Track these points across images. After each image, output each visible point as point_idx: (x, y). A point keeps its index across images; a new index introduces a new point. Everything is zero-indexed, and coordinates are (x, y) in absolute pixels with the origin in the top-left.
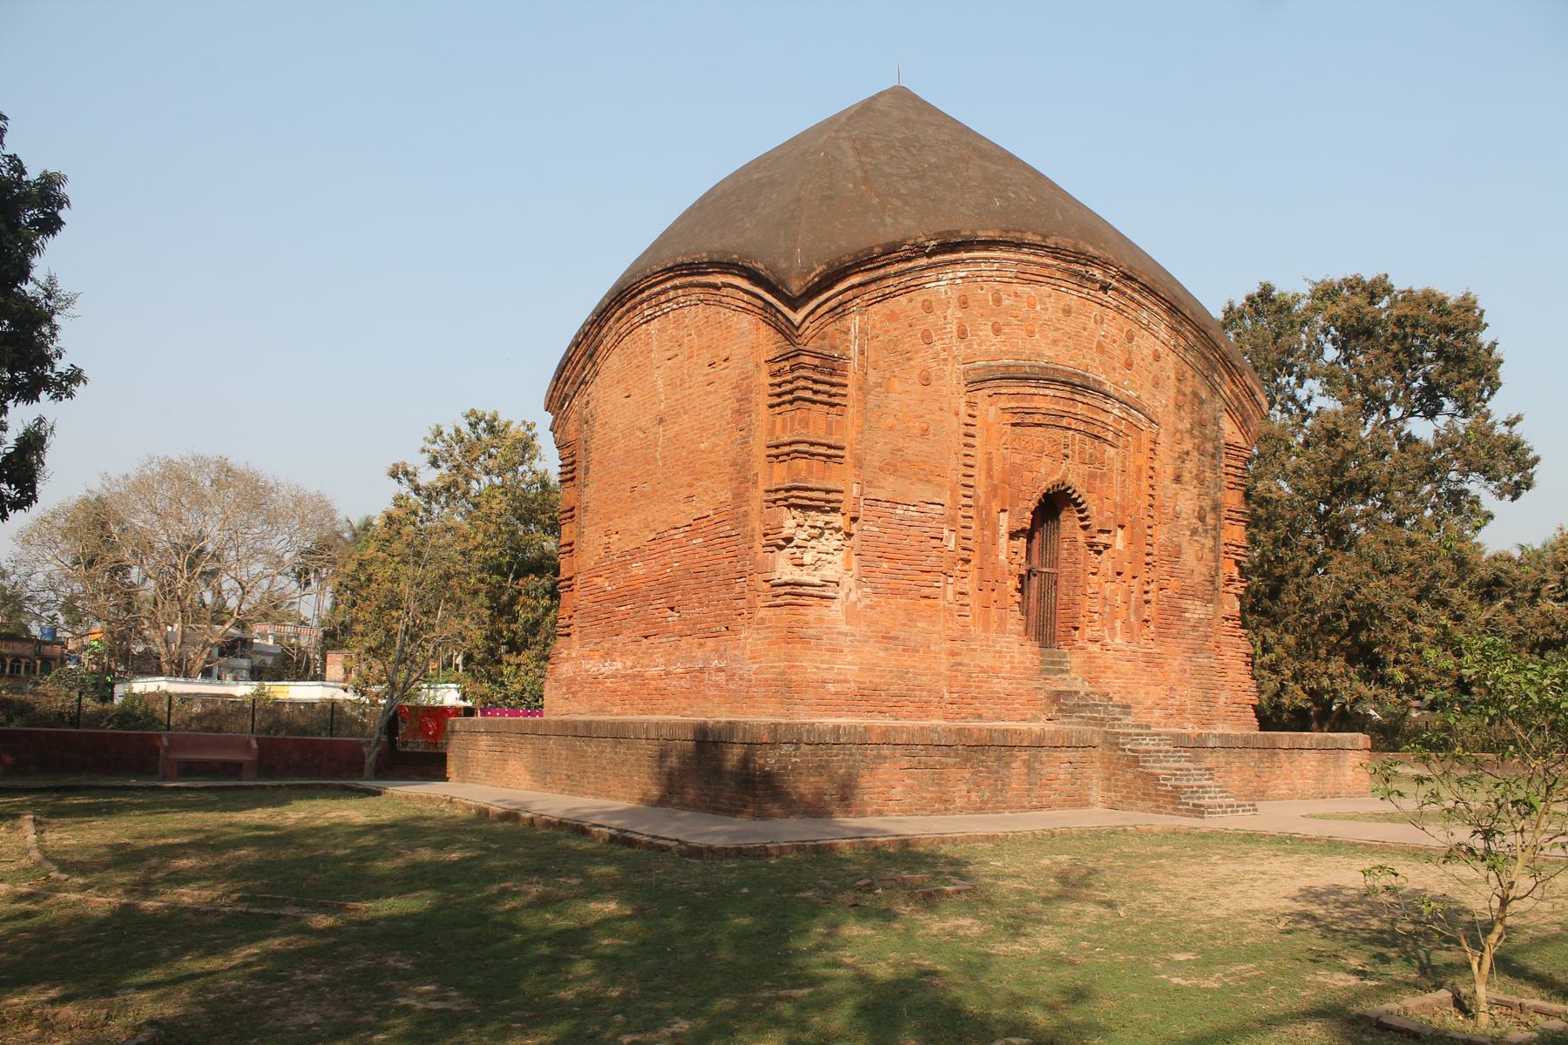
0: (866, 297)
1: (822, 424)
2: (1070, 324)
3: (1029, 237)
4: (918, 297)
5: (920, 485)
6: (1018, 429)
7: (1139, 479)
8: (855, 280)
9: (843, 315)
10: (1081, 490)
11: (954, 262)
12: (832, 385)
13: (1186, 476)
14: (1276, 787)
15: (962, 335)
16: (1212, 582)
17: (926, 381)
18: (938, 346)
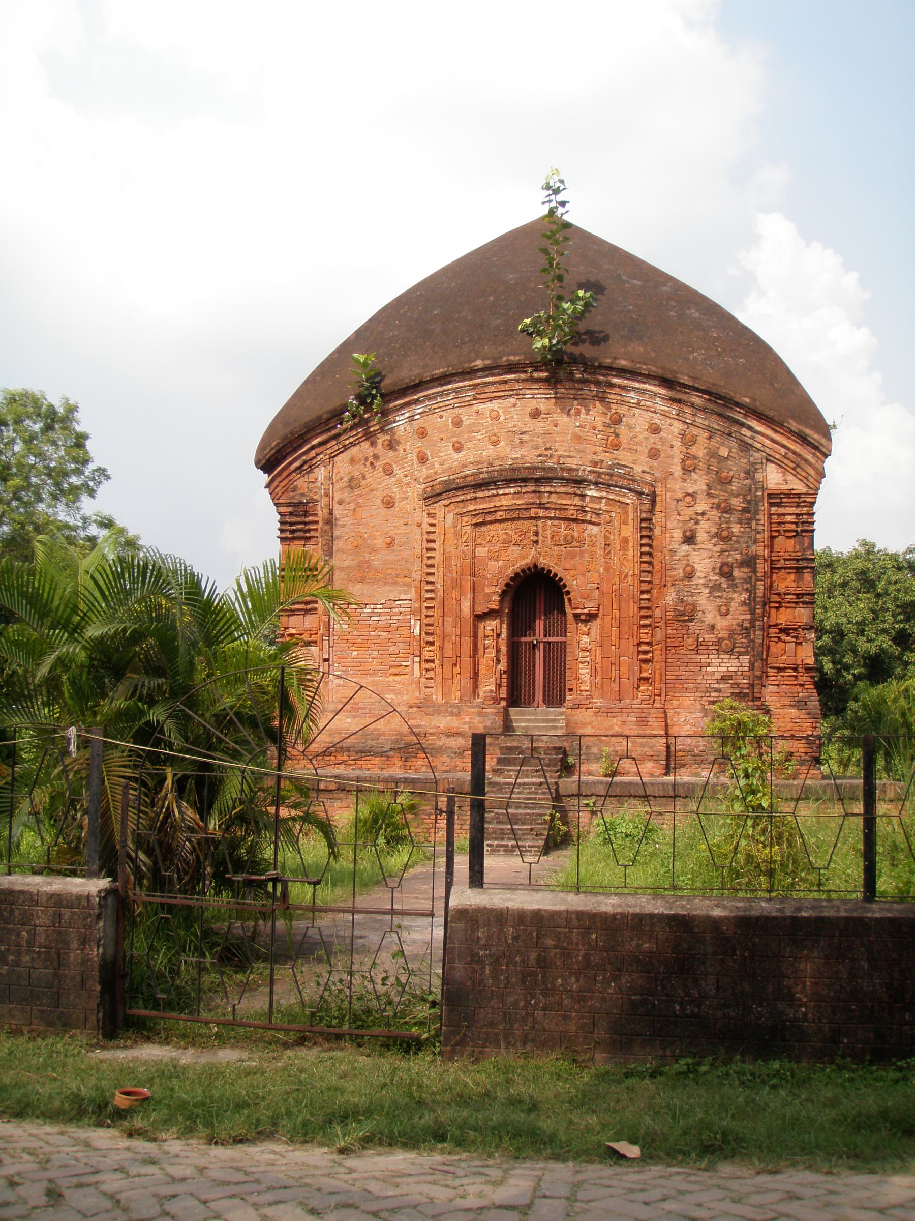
0: (329, 452)
2: (539, 426)
3: (479, 363)
5: (387, 588)
6: (483, 528)
8: (315, 442)
9: (311, 469)
11: (408, 404)
12: (305, 523)
13: (701, 536)
15: (423, 459)
17: (389, 503)
18: (399, 472)
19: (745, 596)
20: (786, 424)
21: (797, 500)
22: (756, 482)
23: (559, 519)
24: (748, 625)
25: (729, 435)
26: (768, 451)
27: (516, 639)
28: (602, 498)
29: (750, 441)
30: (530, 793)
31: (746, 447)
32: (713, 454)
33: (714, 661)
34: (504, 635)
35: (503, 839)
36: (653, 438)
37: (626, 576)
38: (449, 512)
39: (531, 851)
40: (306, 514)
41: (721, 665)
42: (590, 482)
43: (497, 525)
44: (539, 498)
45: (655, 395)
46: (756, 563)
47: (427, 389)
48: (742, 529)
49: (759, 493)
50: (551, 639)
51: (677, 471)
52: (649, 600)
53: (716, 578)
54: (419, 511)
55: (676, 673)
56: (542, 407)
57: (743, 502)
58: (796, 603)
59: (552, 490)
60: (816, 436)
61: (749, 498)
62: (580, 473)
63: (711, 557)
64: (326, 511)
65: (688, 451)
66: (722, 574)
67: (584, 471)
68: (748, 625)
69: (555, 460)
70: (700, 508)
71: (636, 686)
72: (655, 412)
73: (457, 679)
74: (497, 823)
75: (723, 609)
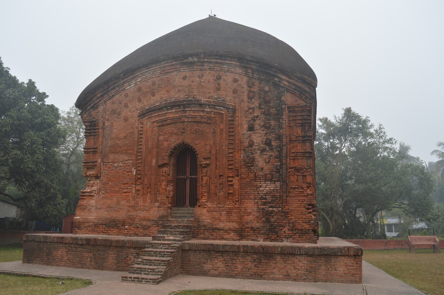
0: (104, 99)
1: (92, 142)
2: (186, 83)
4: (123, 93)
6: (162, 128)
7: (221, 134)
8: (98, 96)
9: (97, 108)
10: (191, 145)
12: (95, 129)
13: (257, 127)
14: (272, 273)
16: (279, 172)
19: (277, 153)
20: (295, 74)
21: (302, 109)
22: (281, 101)
23: (193, 122)
24: (279, 168)
25: (269, 81)
26: (286, 87)
27: (178, 177)
28: (211, 111)
29: (279, 83)
30: (165, 249)
31: (276, 85)
32: (261, 90)
33: (263, 185)
34: (171, 175)
35: (141, 274)
36: (235, 85)
37: (222, 146)
38: (148, 121)
39: (150, 282)
40: (95, 125)
41: (267, 187)
42: (206, 104)
43: (168, 126)
44: (185, 113)
45: (236, 65)
46: (282, 138)
47: (142, 71)
48: (275, 123)
49: (283, 106)
50: (193, 177)
51: (245, 98)
52: (232, 156)
53: (264, 146)
54: (137, 122)
55: (246, 191)
56: (188, 75)
57: (276, 111)
58: (303, 157)
59: (190, 109)
60: (309, 79)
61: (278, 108)
62: (202, 102)
63: (261, 137)
64: (102, 124)
65: (251, 89)
66: (266, 144)
67: (204, 100)
68: (279, 168)
69: (192, 97)
70: (255, 114)
71: (227, 197)
72: (235, 73)
73: (149, 195)
74: (143, 264)
75: (267, 160)
